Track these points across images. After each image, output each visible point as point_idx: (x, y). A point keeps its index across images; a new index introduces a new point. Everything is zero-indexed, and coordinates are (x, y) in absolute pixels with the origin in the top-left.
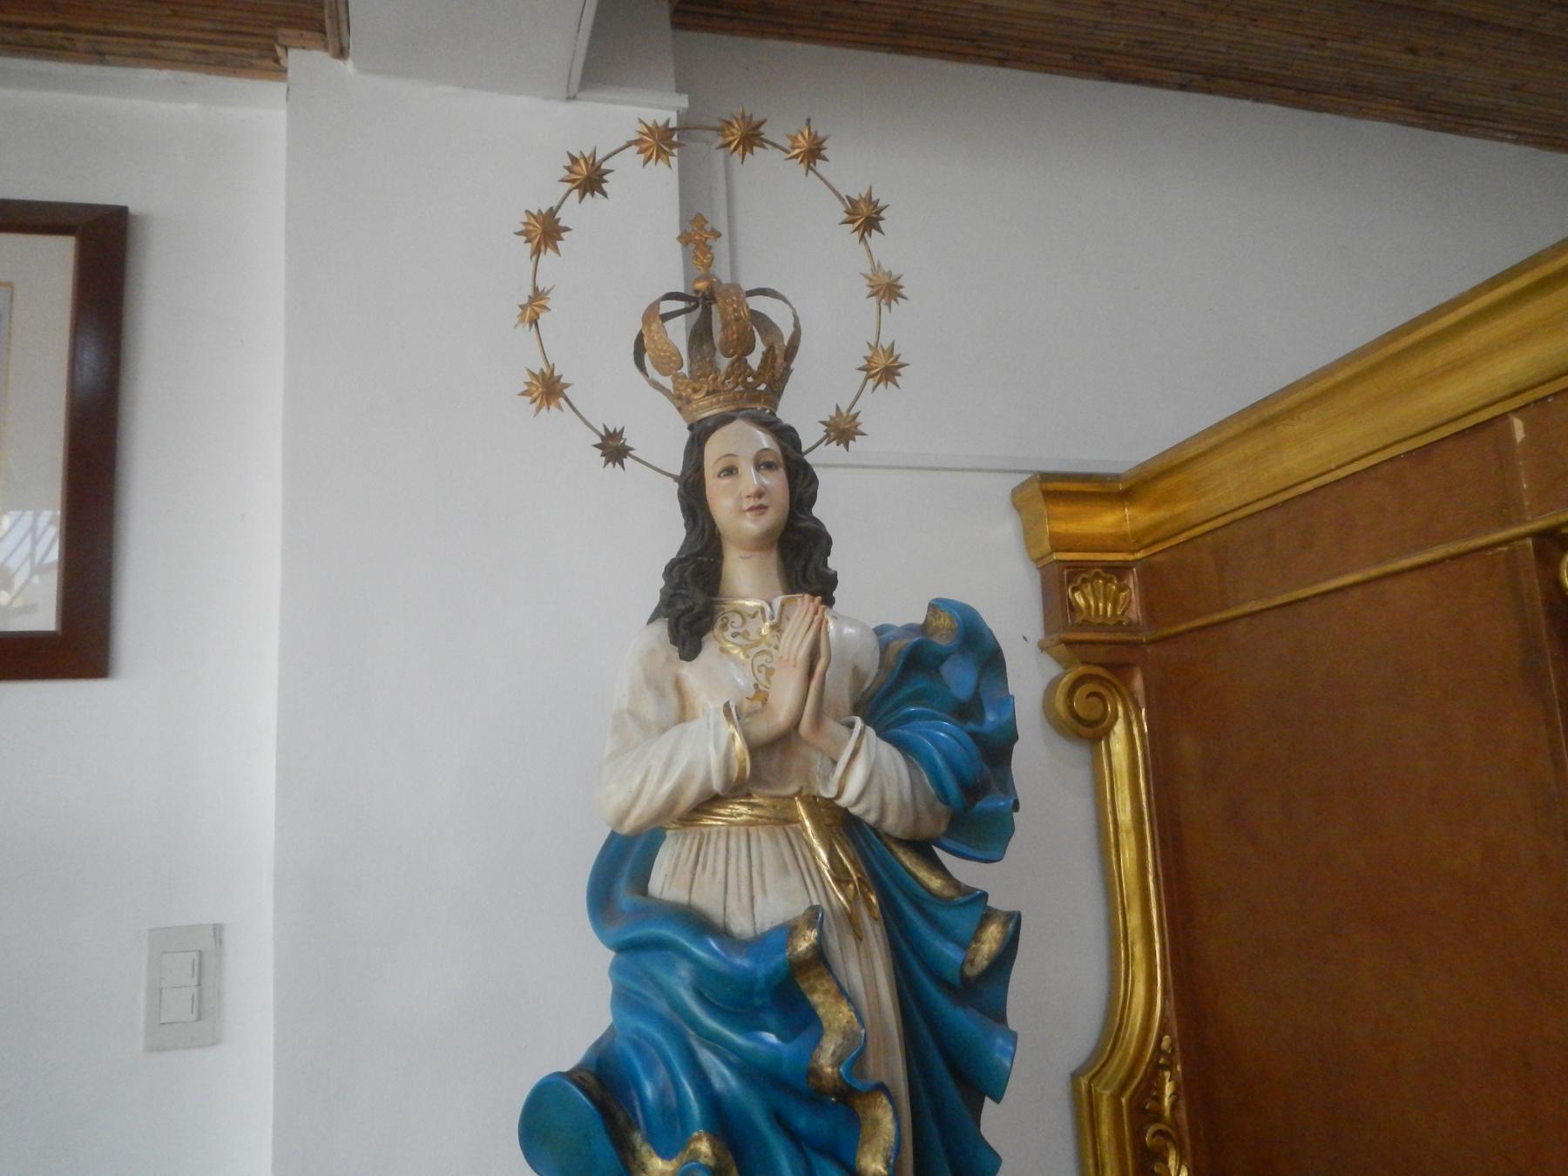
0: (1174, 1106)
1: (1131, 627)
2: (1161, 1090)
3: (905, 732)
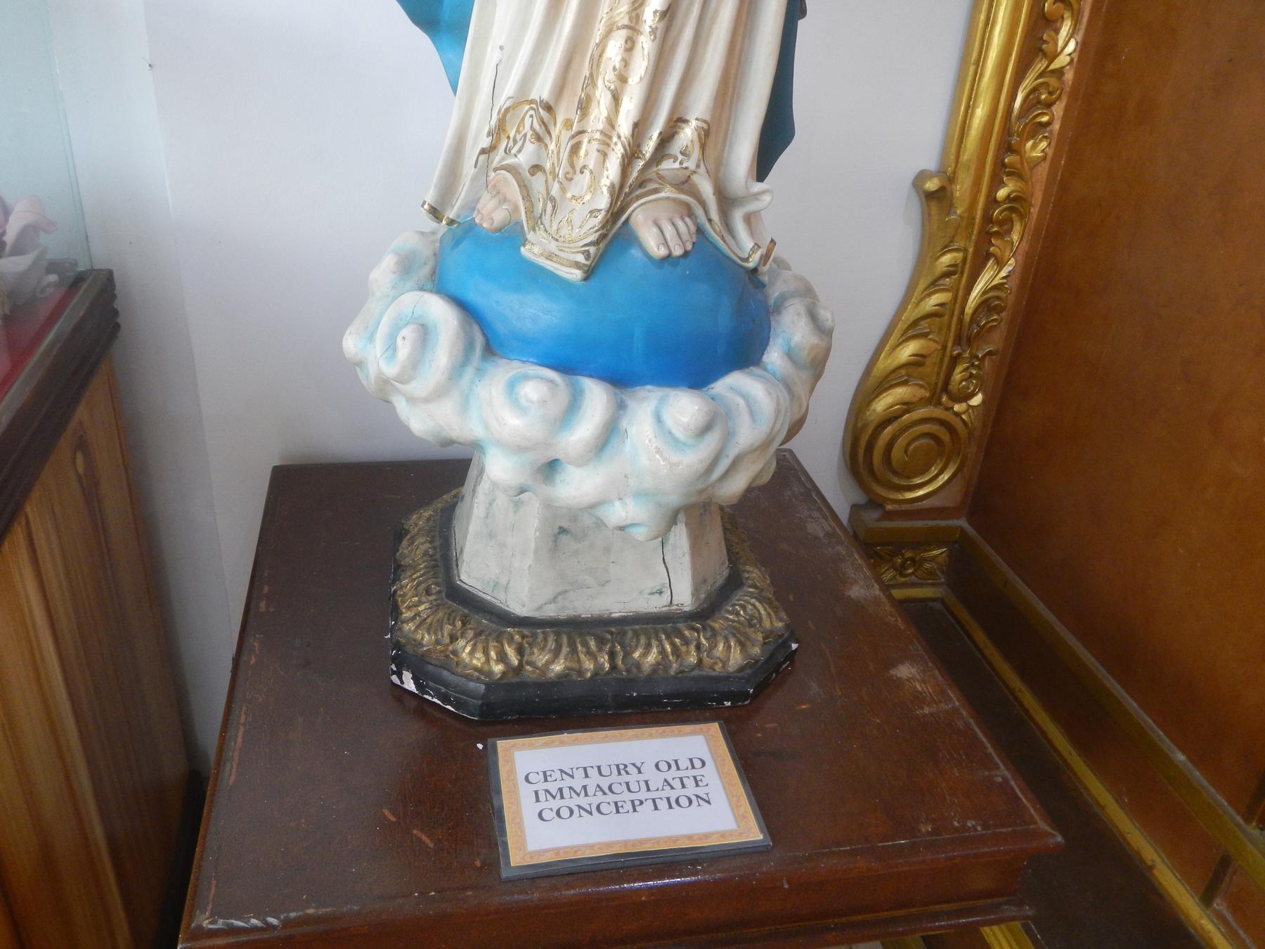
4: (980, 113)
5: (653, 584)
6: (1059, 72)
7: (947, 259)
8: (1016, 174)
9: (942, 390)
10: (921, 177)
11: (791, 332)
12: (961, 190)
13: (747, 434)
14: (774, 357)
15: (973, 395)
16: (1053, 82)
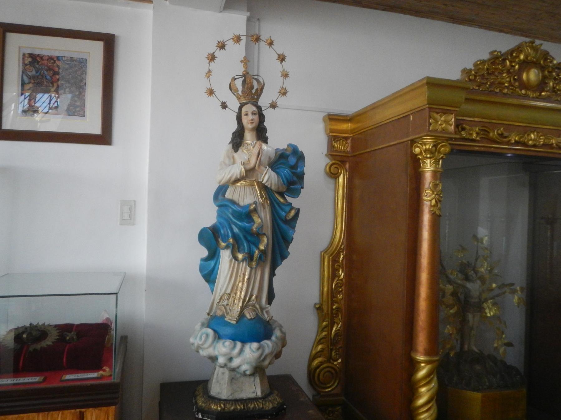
0: (342, 260)
1: (348, 152)
2: (340, 256)
3: (278, 170)
4: (326, 289)
5: (252, 390)
6: (342, 280)
7: (324, 323)
8: (336, 302)
9: (330, 359)
10: (315, 304)
11: (277, 333)
12: (325, 308)
13: (267, 351)
14: (273, 338)
15: (338, 360)
16: (340, 282)
